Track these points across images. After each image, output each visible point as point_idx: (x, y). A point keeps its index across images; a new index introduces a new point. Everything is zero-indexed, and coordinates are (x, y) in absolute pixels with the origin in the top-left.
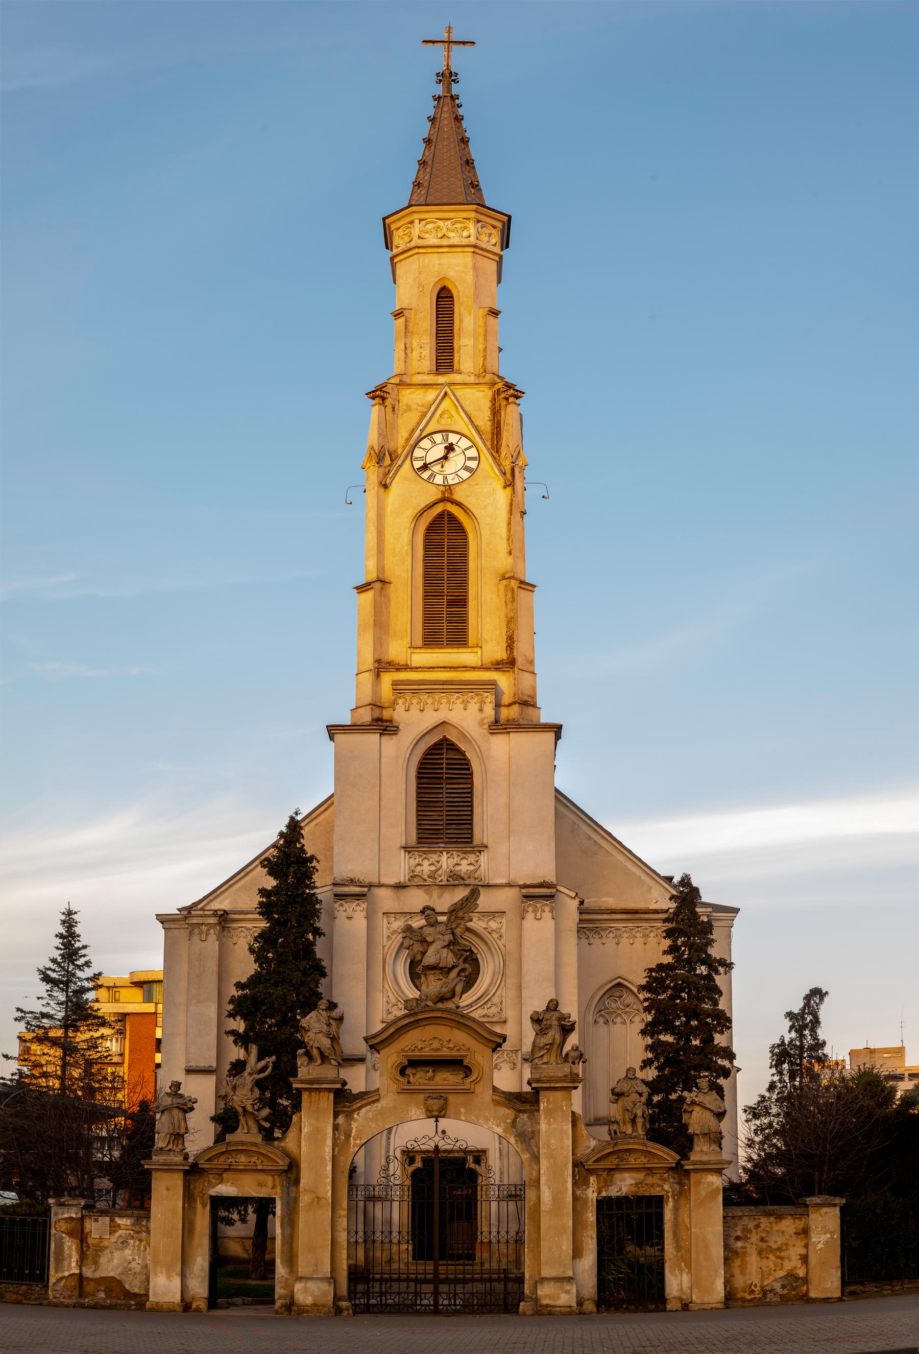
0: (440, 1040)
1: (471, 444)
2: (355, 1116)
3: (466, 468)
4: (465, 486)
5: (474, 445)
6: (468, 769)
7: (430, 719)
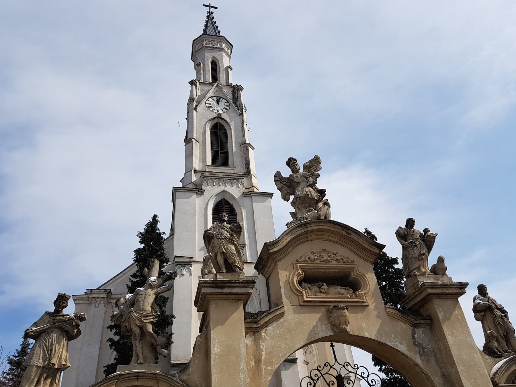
1: (226, 101)
2: (263, 334)
3: (226, 109)
5: (228, 102)
6: (235, 212)
7: (218, 189)
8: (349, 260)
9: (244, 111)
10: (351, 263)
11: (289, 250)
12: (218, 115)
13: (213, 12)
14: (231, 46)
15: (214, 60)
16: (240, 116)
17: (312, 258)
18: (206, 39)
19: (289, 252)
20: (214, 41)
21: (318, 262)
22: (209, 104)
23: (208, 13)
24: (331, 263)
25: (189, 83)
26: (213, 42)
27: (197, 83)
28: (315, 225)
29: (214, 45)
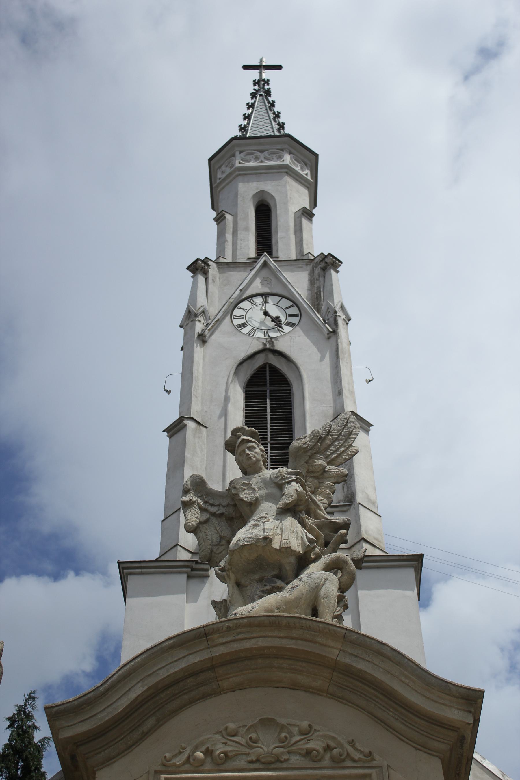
0: (282, 728)
1: (291, 304)
4: (287, 338)
5: (295, 303)
8: (356, 749)
9: (340, 322)
10: (359, 760)
11: (145, 728)
12: (265, 345)
13: (268, 80)
14: (314, 157)
15: (262, 201)
16: (329, 338)
17: (219, 749)
18: (242, 149)
19: (145, 736)
20: (262, 151)
21: (241, 762)
22: (241, 317)
23: (255, 85)
24: (284, 765)
25: (188, 268)
26: (258, 154)
27: (208, 265)
28: (240, 636)
29: (262, 162)
